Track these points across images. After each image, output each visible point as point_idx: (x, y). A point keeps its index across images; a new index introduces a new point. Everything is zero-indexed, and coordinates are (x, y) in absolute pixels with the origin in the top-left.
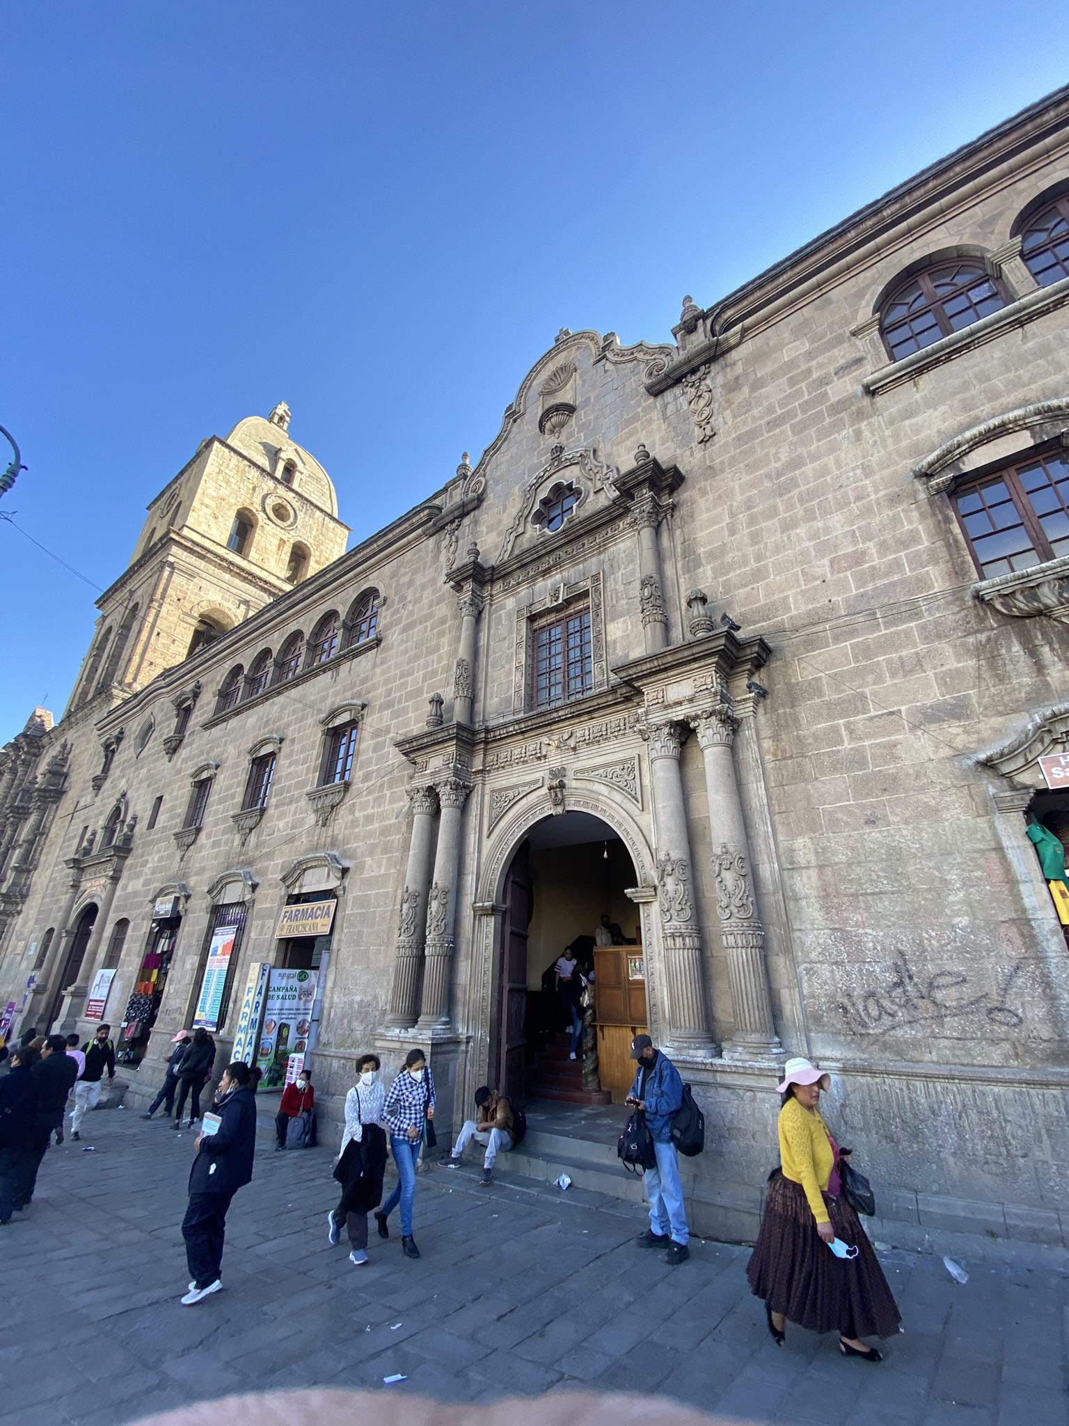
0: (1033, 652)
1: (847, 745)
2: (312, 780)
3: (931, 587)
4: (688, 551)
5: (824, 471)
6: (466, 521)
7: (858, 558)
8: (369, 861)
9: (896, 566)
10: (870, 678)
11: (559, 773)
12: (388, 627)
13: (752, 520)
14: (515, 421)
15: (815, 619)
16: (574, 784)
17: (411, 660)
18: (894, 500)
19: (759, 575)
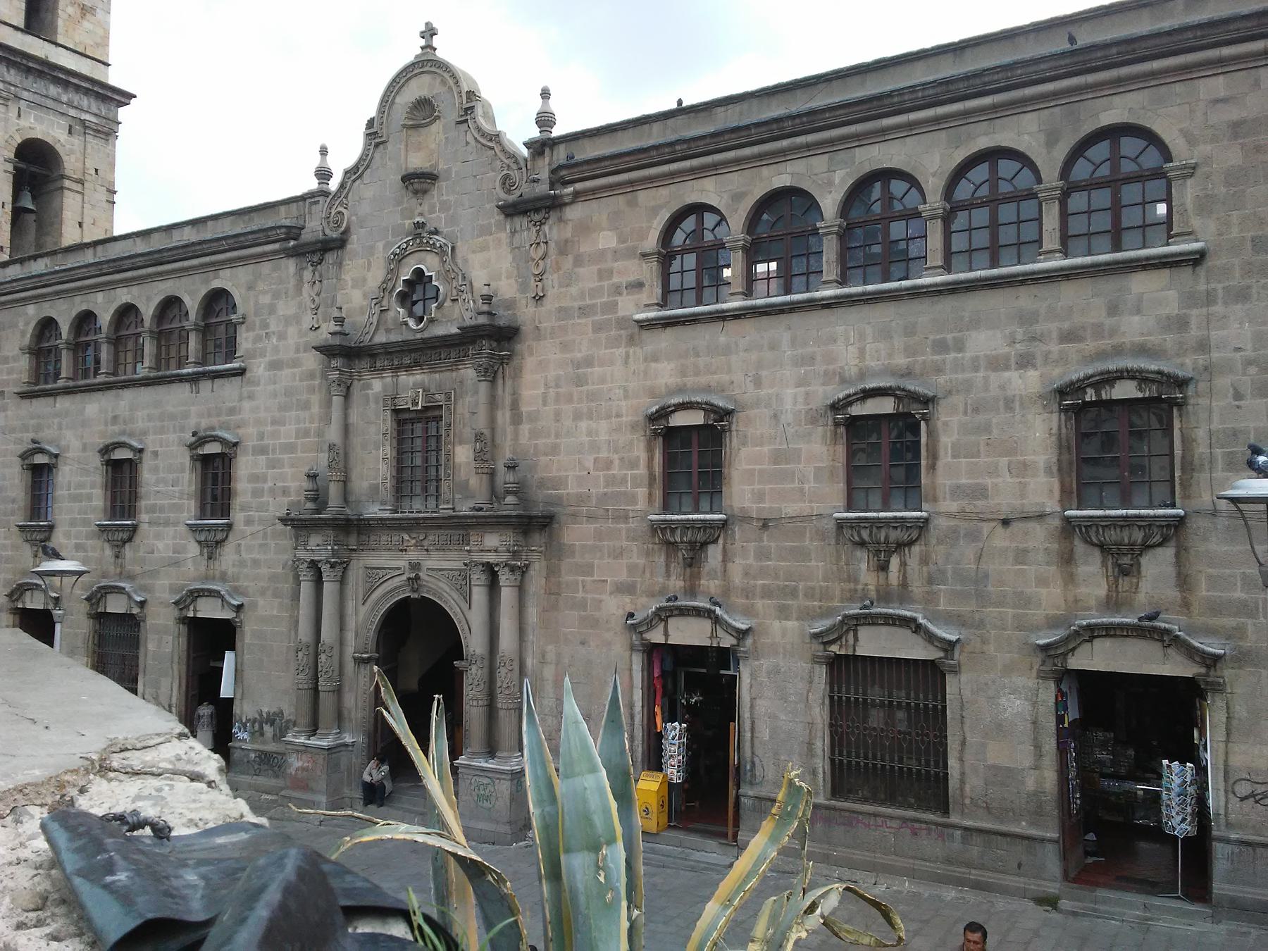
0: (668, 566)
1: (580, 595)
2: (189, 511)
3: (637, 504)
4: (515, 406)
5: (603, 380)
6: (330, 257)
7: (608, 464)
8: (261, 602)
9: (623, 481)
10: (598, 555)
11: (415, 566)
12: (252, 354)
13: (557, 400)
14: (377, 145)
15: (582, 499)
16: (427, 578)
17: (282, 408)
18: (634, 427)
19: (554, 450)
